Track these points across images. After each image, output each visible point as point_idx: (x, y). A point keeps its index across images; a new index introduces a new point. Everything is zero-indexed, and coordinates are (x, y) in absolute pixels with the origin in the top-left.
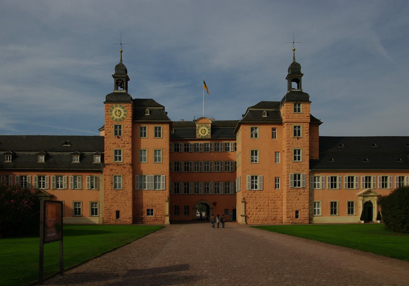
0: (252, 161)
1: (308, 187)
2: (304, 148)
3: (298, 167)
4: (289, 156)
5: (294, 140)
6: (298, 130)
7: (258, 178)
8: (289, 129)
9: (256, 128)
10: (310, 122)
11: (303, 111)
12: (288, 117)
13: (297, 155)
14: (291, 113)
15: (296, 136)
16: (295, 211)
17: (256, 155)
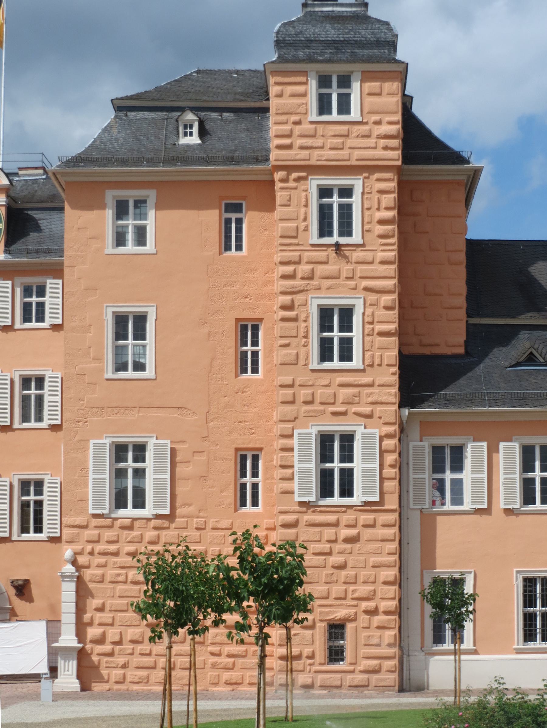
0: (121, 367)
1: (392, 503)
2: (372, 297)
3: (340, 399)
4: (294, 341)
5: (321, 255)
6: (341, 206)
7: (149, 455)
8: (294, 202)
9: (140, 203)
10: (399, 163)
11: (366, 110)
12: (287, 141)
13: (336, 334)
14: (298, 123)
15: (330, 234)
16: (324, 624)
17: (140, 334)
